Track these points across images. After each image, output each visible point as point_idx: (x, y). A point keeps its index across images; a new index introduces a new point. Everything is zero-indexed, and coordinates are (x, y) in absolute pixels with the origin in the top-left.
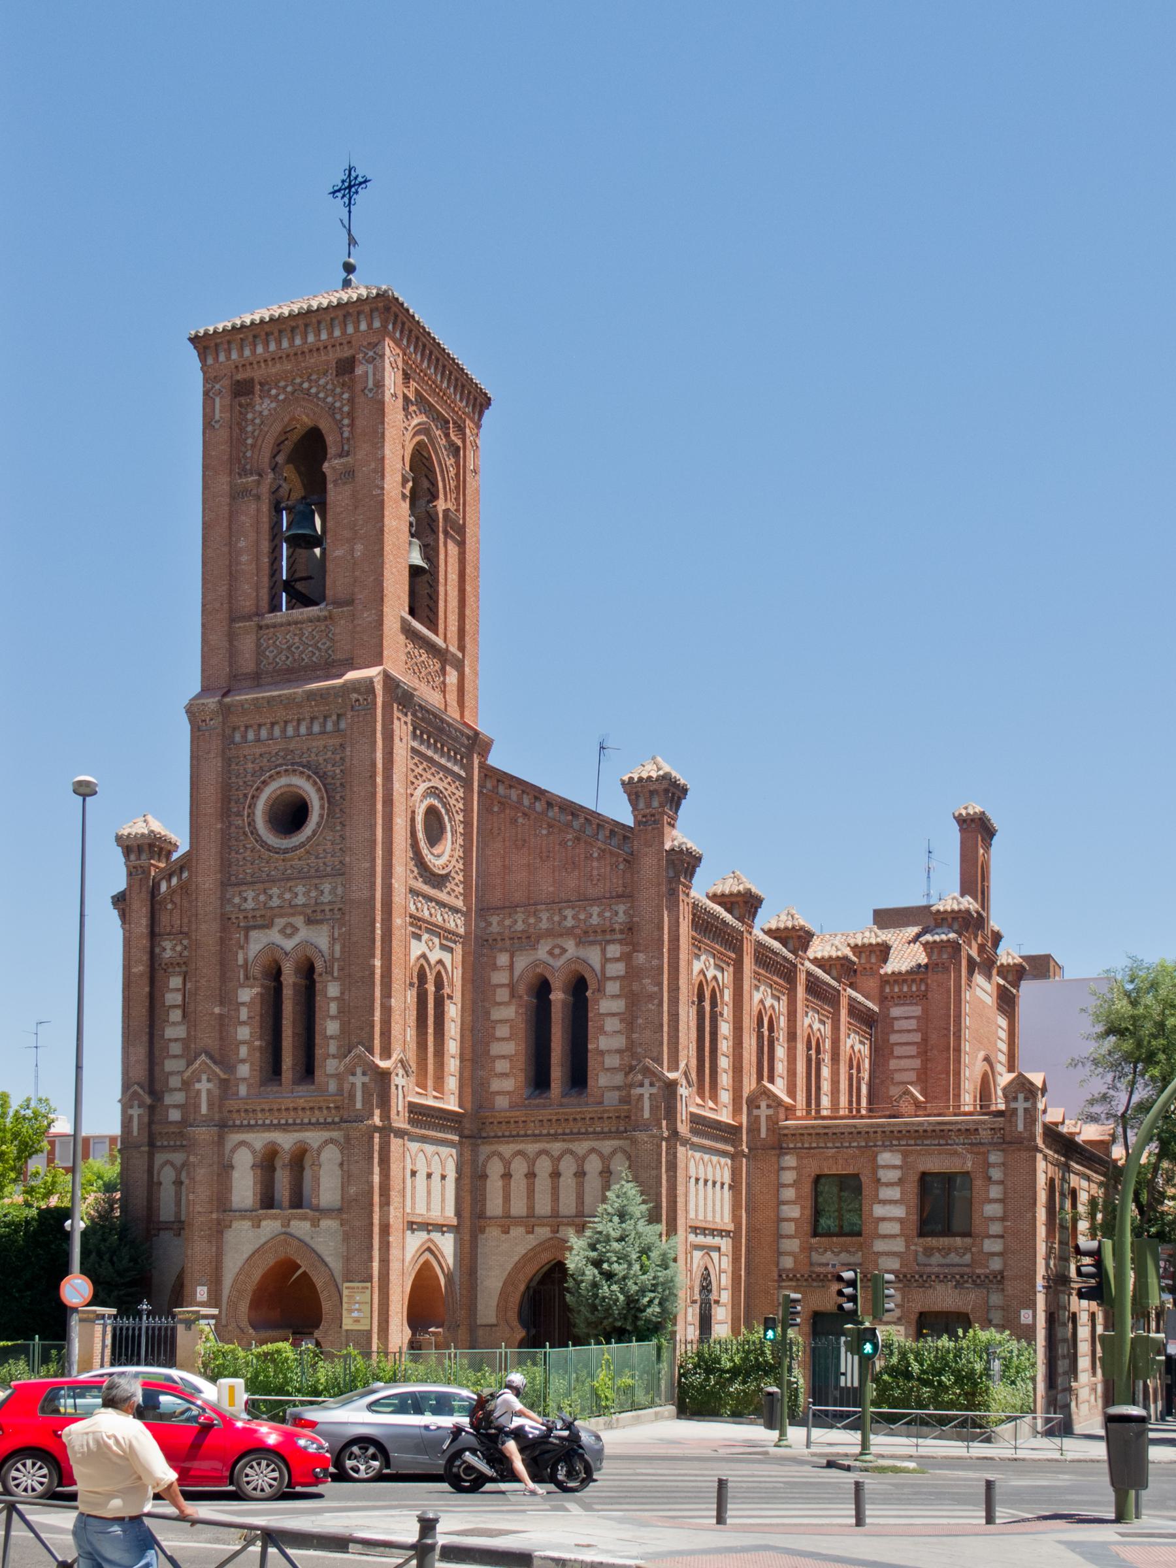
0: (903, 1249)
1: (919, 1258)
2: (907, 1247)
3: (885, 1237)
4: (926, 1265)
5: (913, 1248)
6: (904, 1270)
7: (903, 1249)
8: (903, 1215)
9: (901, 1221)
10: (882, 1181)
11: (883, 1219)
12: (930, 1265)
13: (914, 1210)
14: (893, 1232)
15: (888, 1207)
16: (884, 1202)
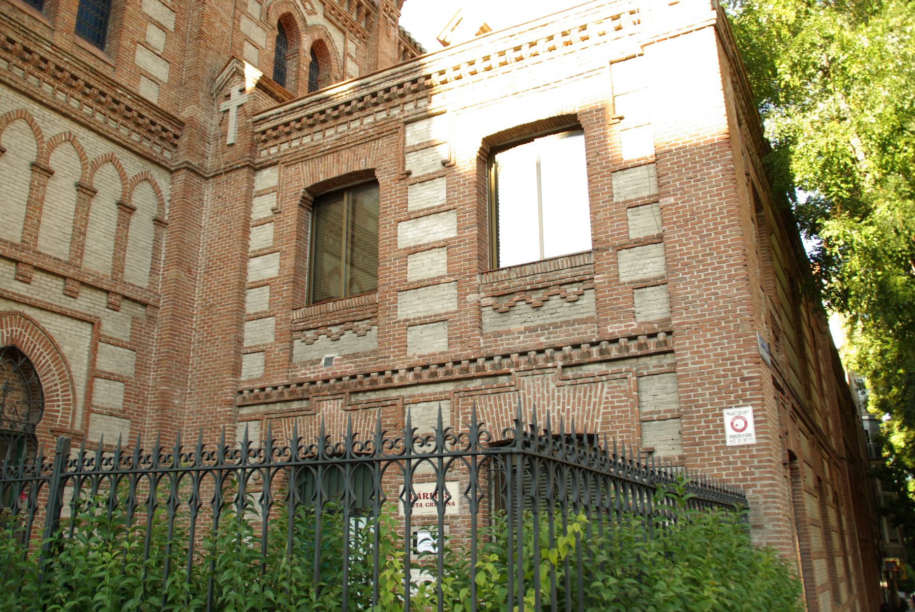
0: (452, 306)
1: (486, 320)
2: (461, 298)
3: (418, 286)
4: (498, 334)
5: (472, 298)
6: (458, 351)
7: (452, 306)
8: (453, 234)
9: (445, 245)
10: (414, 175)
11: (416, 250)
12: (508, 332)
13: (472, 218)
14: (433, 273)
15: (424, 223)
16: (417, 216)
